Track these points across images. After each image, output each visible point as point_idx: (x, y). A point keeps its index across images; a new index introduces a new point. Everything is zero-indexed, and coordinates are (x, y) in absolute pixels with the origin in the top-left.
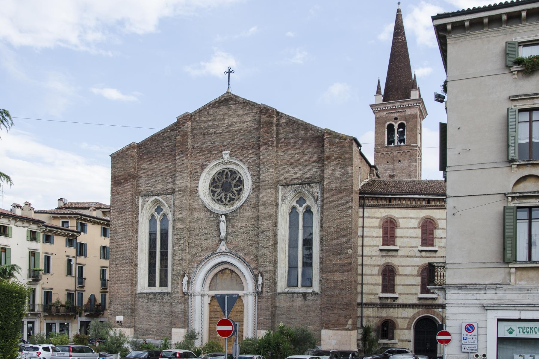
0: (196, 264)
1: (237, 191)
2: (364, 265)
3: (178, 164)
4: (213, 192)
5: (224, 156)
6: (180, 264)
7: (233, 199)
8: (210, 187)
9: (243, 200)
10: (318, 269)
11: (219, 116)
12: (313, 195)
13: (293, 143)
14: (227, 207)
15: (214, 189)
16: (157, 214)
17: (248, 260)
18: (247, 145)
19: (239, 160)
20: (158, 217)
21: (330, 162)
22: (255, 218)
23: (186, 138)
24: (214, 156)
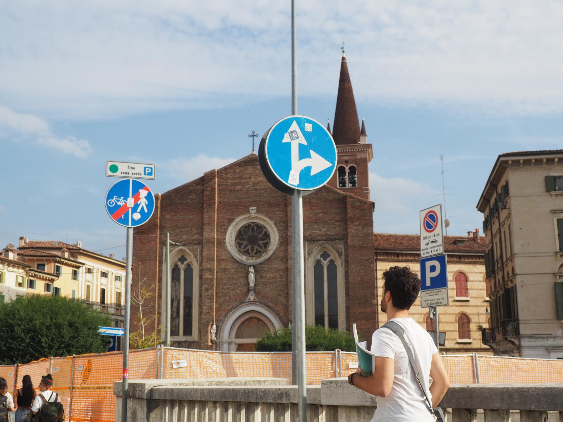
0: (224, 313)
1: (263, 244)
2: (379, 314)
3: (206, 217)
4: (239, 245)
5: (251, 211)
6: (209, 313)
7: (260, 252)
8: (236, 239)
9: (270, 253)
10: (345, 318)
11: (245, 175)
12: (337, 250)
13: (316, 203)
14: (254, 258)
15: (240, 242)
16: (180, 263)
17: (278, 309)
18: (273, 203)
19: (266, 216)
20: (182, 267)
21: (353, 222)
22: (283, 269)
23: (213, 193)
24: (241, 211)
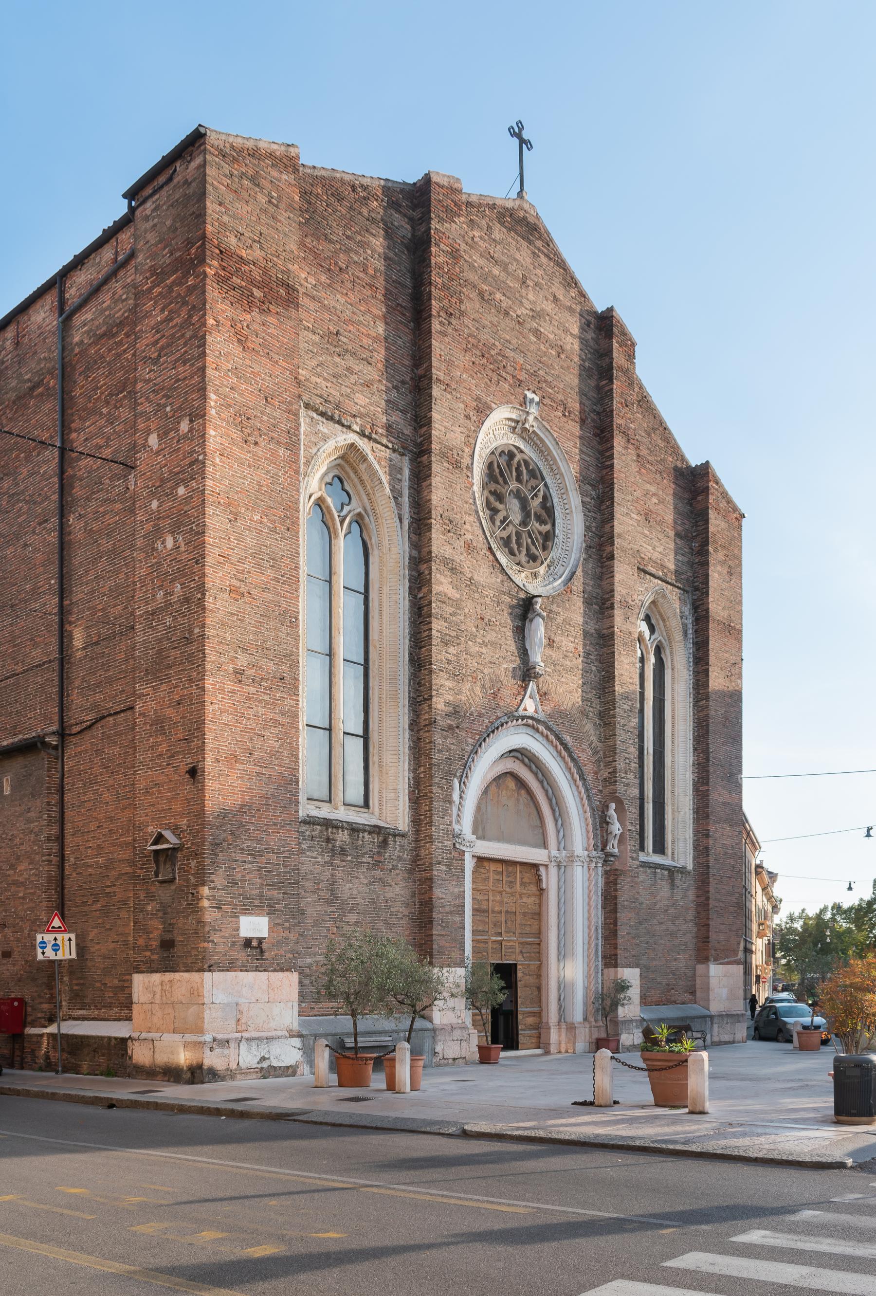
6: (450, 728)
15: (492, 499)
